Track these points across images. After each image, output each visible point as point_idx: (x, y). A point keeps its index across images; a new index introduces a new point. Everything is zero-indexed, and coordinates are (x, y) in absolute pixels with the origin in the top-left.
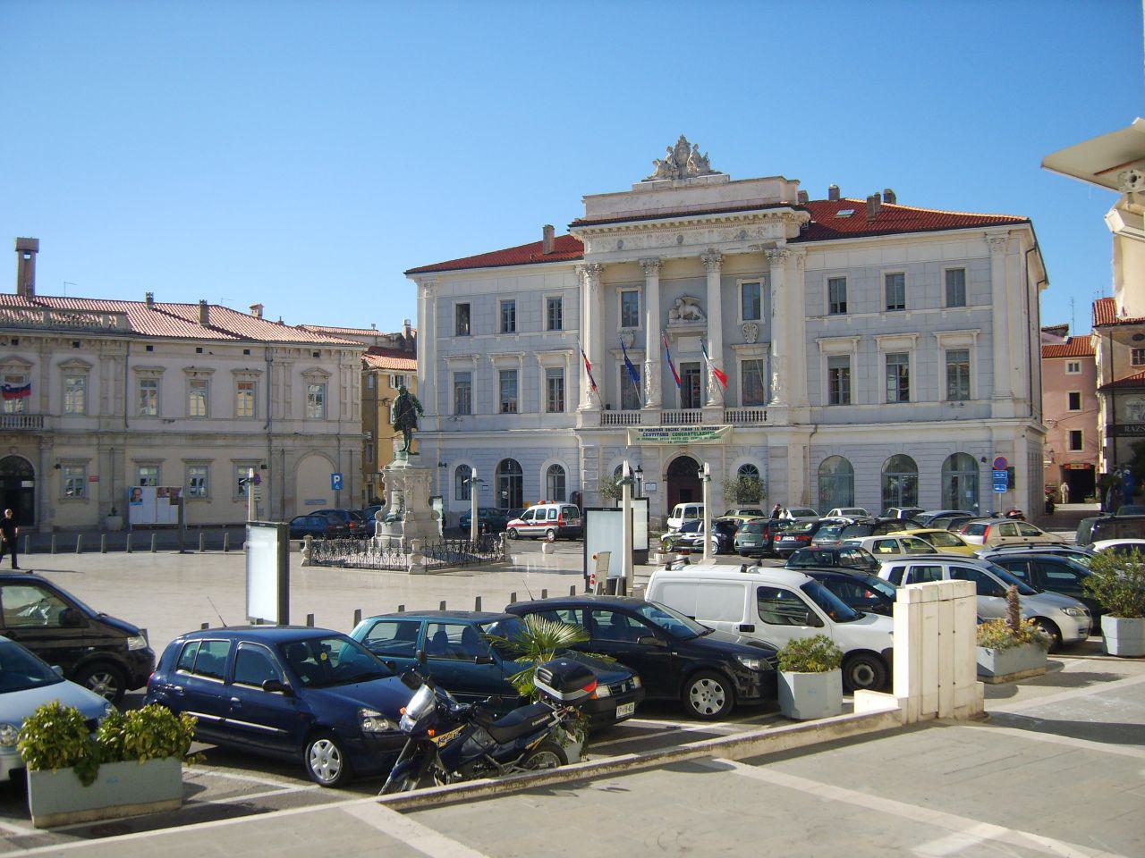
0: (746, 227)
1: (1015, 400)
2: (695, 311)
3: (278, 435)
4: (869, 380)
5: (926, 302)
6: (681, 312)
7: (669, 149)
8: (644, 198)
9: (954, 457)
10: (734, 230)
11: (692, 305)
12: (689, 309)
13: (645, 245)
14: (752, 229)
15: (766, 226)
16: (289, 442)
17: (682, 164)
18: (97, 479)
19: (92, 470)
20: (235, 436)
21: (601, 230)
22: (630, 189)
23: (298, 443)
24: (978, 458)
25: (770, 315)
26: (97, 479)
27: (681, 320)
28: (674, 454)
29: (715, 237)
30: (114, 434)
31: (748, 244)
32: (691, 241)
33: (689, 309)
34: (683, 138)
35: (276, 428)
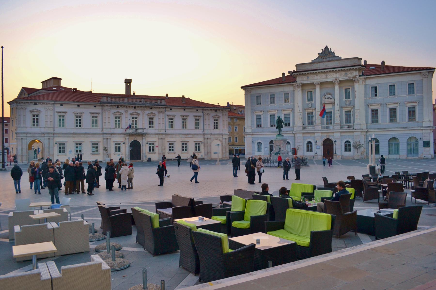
1: (430, 121)
2: (330, 96)
3: (206, 134)
4: (384, 115)
5: (384, 93)
6: (326, 97)
7: (322, 50)
9: (411, 138)
10: (343, 73)
12: (328, 96)
14: (349, 73)
16: (209, 136)
18: (157, 147)
19: (156, 144)
20: (195, 134)
21: (303, 74)
22: (311, 62)
23: (212, 136)
24: (418, 138)
25: (354, 98)
26: (157, 147)
27: (326, 99)
30: (162, 134)
33: (328, 96)
35: (206, 132)
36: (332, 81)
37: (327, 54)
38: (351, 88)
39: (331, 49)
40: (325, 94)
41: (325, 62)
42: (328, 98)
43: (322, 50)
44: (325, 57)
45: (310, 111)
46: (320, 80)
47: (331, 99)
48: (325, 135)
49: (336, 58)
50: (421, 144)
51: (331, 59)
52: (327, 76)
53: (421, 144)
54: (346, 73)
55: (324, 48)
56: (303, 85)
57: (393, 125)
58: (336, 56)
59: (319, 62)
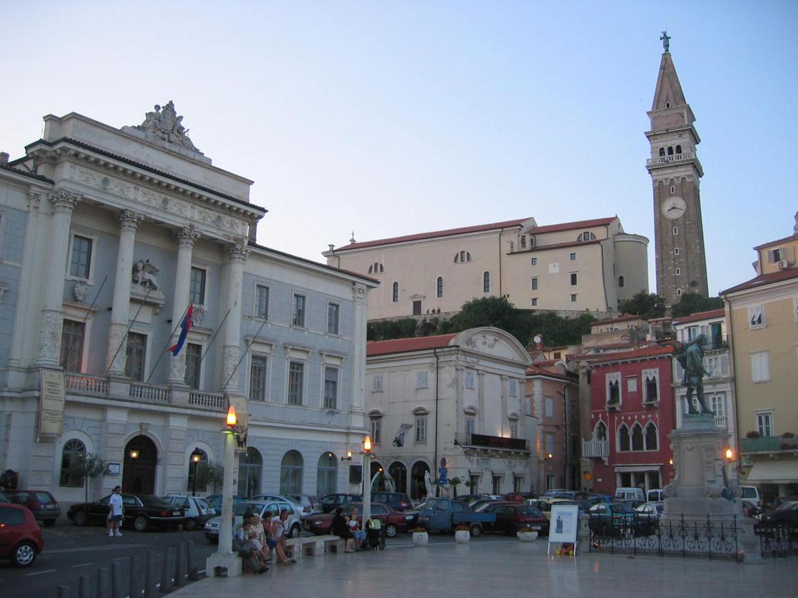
0: (222, 215)
6: (140, 275)
8: (135, 146)
10: (213, 215)
11: (149, 273)
12: (148, 276)
13: (132, 197)
14: (227, 219)
15: (237, 221)
17: (165, 126)
24: (339, 457)
28: (134, 432)
29: (196, 217)
31: (221, 233)
32: (175, 210)
34: (171, 102)
36: (181, 229)
37: (165, 126)
38: (208, 269)
39: (181, 118)
40: (140, 265)
41: (170, 153)
42: (144, 283)
43: (157, 107)
44: (166, 136)
45: (77, 315)
46: (144, 209)
47: (154, 288)
48: (138, 420)
49: (198, 157)
50: (343, 473)
51: (184, 152)
52: (165, 201)
53: (343, 473)
54: (219, 218)
55: (163, 104)
56: (84, 207)
57: (295, 414)
58: (197, 151)
59: (151, 145)
